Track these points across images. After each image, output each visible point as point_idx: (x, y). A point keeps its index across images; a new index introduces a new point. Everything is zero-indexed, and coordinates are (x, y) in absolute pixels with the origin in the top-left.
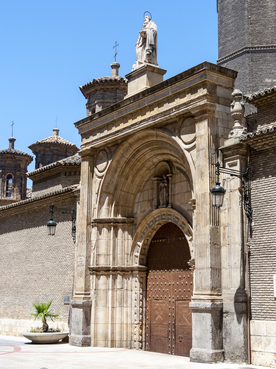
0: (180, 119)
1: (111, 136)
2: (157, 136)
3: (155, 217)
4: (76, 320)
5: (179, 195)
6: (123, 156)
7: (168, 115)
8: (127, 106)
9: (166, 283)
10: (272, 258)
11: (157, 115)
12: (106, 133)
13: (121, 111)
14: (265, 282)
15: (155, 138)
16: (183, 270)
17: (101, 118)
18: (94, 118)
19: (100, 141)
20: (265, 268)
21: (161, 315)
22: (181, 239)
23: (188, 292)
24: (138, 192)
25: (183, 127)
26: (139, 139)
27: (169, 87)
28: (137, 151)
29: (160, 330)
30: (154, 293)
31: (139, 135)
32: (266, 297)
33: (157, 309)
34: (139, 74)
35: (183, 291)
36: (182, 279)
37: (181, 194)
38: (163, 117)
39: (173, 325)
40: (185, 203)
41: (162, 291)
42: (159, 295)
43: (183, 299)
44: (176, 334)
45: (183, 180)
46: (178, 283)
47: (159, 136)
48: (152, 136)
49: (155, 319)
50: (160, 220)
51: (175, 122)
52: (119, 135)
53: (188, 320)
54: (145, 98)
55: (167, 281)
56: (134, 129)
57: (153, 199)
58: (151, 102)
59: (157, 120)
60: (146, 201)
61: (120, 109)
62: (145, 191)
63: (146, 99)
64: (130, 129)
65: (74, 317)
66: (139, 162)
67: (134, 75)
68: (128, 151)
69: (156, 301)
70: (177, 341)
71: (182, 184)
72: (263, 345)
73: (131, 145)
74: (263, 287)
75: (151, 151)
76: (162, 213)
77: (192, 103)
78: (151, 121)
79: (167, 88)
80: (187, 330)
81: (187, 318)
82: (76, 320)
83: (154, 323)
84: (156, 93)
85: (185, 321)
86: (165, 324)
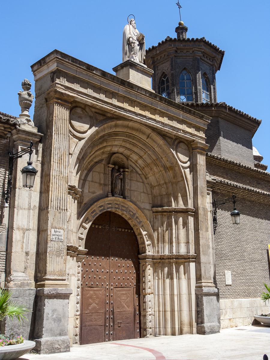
0: (176, 139)
1: (110, 106)
2: (148, 137)
3: (107, 203)
4: (55, 316)
5: (135, 193)
6: (104, 130)
7: (176, 131)
8: (139, 94)
9: (103, 270)
10: (223, 260)
11: (168, 125)
12: (102, 97)
13: (129, 92)
14: (221, 275)
15: (144, 137)
16: (127, 259)
17: (103, 79)
18: (94, 72)
19: (92, 99)
20: (220, 266)
21: (96, 303)
22: (120, 230)
23: (127, 280)
24: (86, 169)
25: (180, 147)
26: (127, 127)
27: (182, 112)
28: (114, 134)
29: (95, 319)
30: (87, 280)
31: (131, 124)
32: (221, 284)
33: (91, 297)
34: (143, 71)
35: (122, 279)
36: (121, 268)
37: (138, 192)
38: (172, 130)
39: (110, 311)
40: (141, 201)
41: (98, 278)
42: (94, 282)
43: (122, 286)
44: (115, 320)
45: (139, 181)
46: (117, 271)
47: (150, 138)
48: (144, 133)
49: (88, 308)
50: (112, 208)
51: (172, 138)
52: (144, 120)
53: (127, 306)
54: (160, 103)
55: (104, 268)
56: (141, 119)
57: (105, 185)
58: (162, 109)
59: (165, 128)
60: (96, 182)
61: (130, 90)
62: (94, 172)
63: (160, 104)
64: (137, 117)
65: (50, 312)
66: (107, 143)
67: (139, 68)
68: (111, 129)
69: (89, 288)
70: (116, 327)
71: (139, 184)
72: (223, 315)
73: (116, 126)
74: (220, 278)
75: (123, 141)
76: (115, 202)
77: (195, 137)
78: (160, 125)
79: (180, 111)
80: (126, 315)
81: (125, 304)
82: (55, 316)
83: (86, 312)
84: (170, 107)
85: (124, 307)
86: (102, 312)
